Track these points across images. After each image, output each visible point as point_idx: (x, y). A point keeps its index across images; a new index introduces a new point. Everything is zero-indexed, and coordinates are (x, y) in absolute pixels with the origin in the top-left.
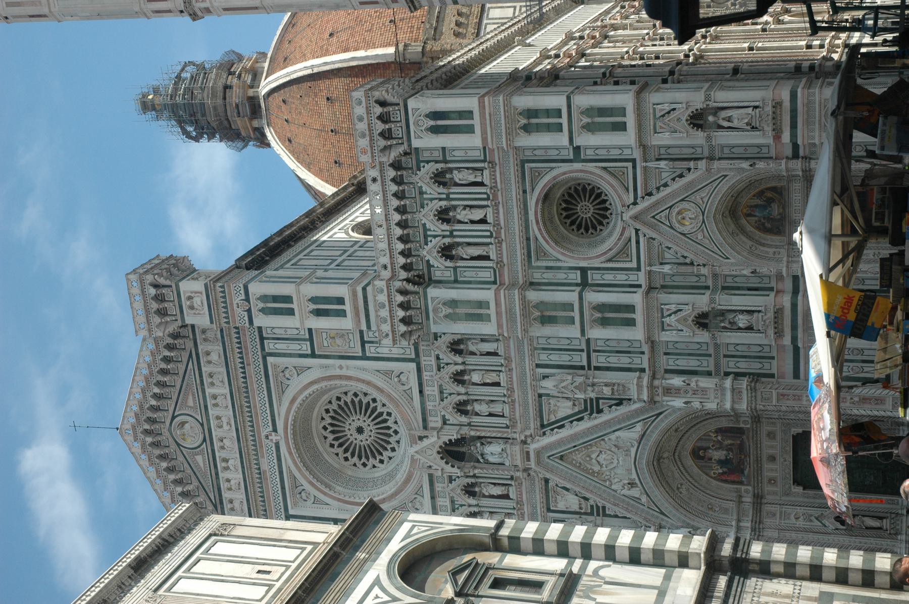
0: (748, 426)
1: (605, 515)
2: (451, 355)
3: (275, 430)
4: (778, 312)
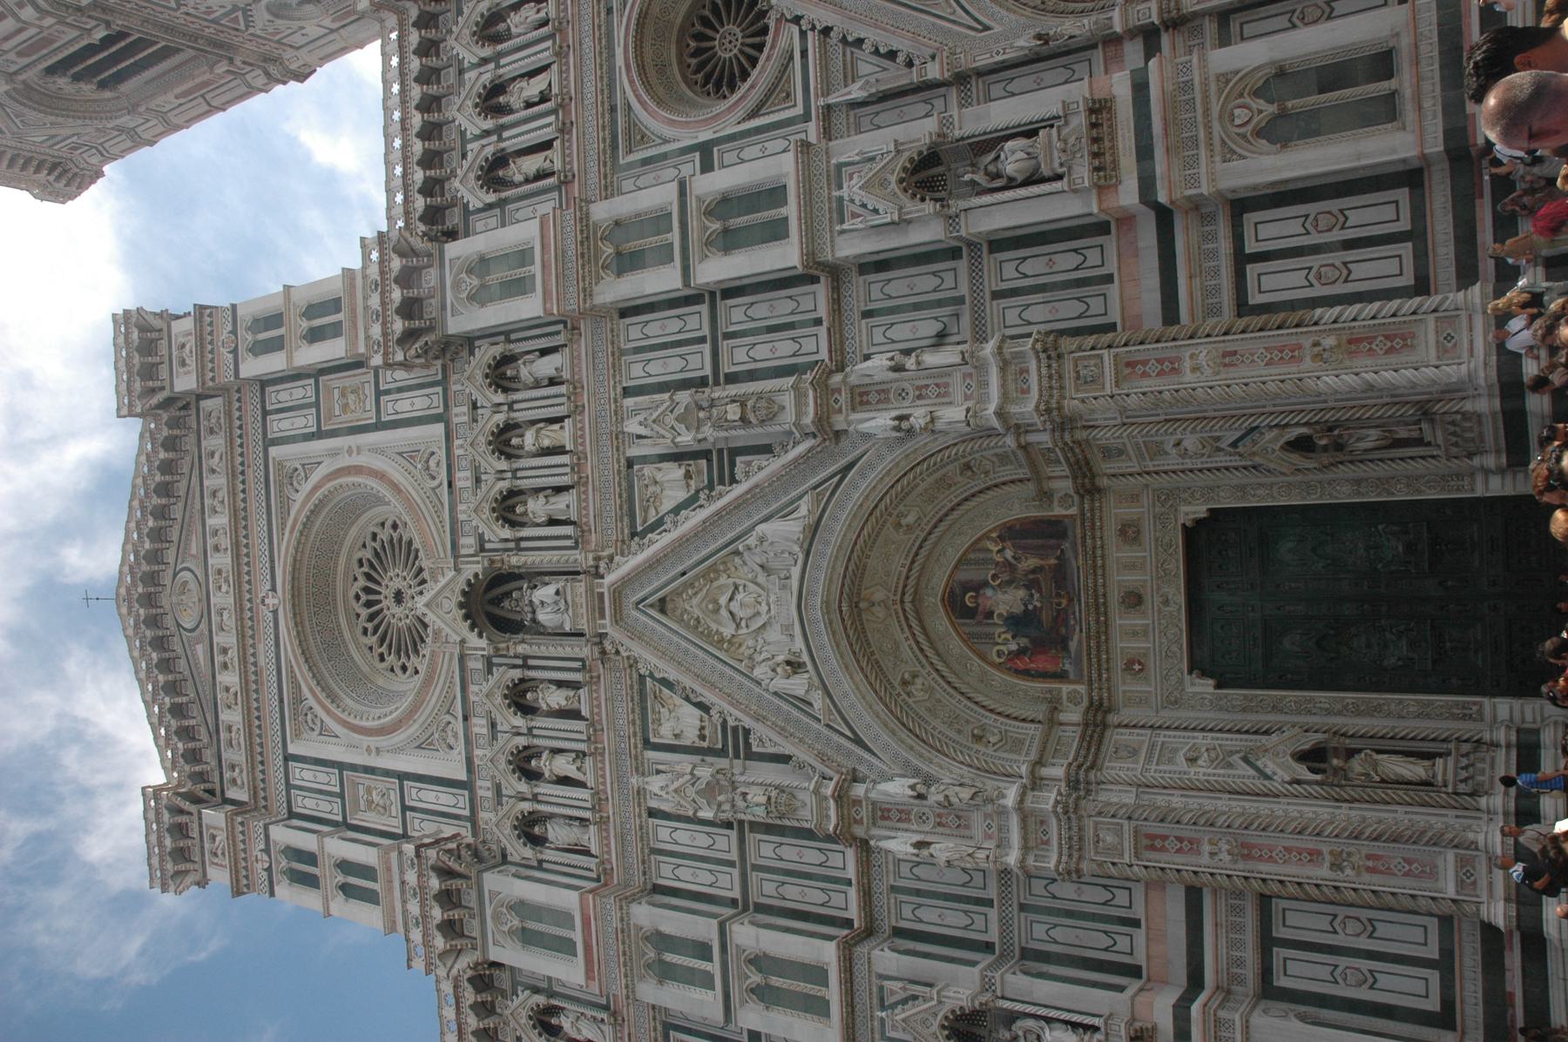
0: (1073, 511)
1: (750, 756)
2: (489, 393)
3: (274, 589)
4: (1099, 109)
